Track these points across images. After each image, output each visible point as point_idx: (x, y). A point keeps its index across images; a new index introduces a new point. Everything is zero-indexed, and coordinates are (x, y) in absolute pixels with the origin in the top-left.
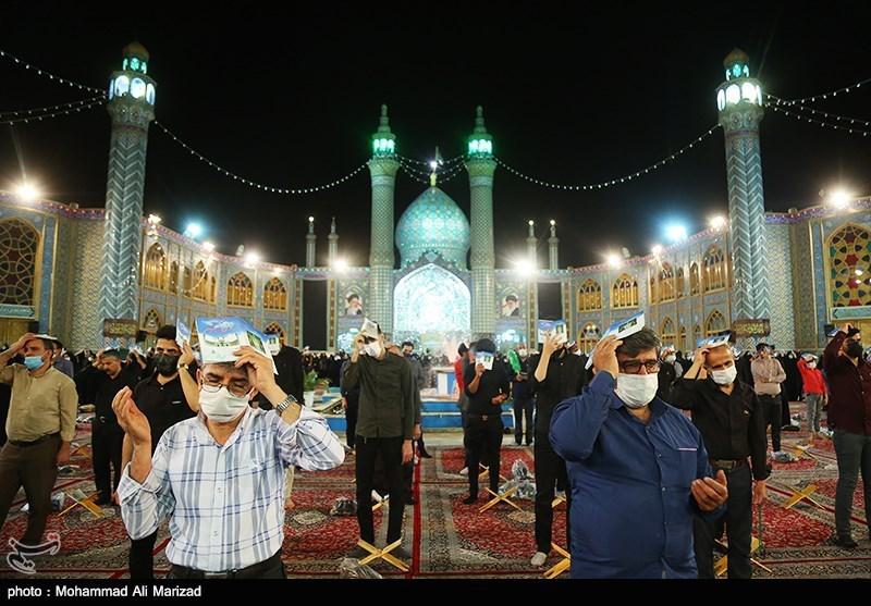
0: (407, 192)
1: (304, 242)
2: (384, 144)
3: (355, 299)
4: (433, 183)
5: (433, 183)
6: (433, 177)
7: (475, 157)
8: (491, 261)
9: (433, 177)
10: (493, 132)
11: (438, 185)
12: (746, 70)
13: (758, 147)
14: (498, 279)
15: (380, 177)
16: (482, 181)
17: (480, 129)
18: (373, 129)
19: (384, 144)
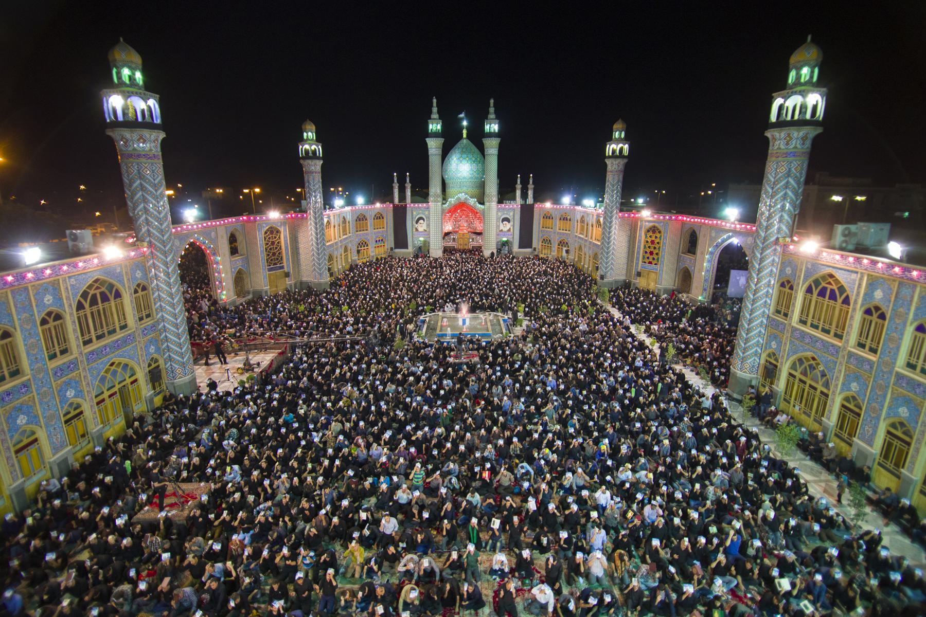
0: (450, 141)
1: (392, 188)
2: (435, 126)
3: (421, 221)
4: (465, 136)
5: (465, 136)
6: (465, 132)
7: (491, 135)
8: (495, 199)
9: (465, 132)
10: (499, 117)
11: (468, 137)
12: (623, 133)
13: (621, 179)
14: (498, 210)
15: (434, 146)
16: (492, 147)
17: (492, 116)
18: (428, 116)
19: (435, 126)
